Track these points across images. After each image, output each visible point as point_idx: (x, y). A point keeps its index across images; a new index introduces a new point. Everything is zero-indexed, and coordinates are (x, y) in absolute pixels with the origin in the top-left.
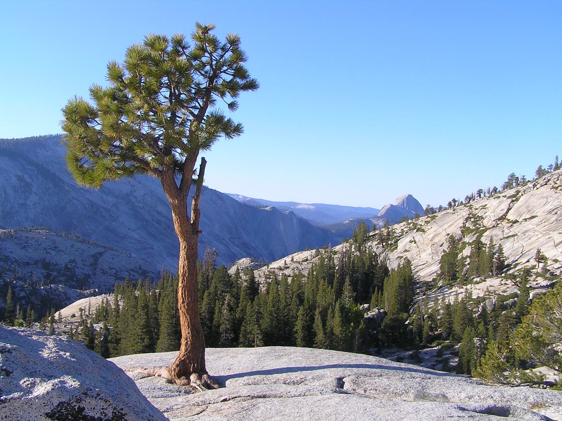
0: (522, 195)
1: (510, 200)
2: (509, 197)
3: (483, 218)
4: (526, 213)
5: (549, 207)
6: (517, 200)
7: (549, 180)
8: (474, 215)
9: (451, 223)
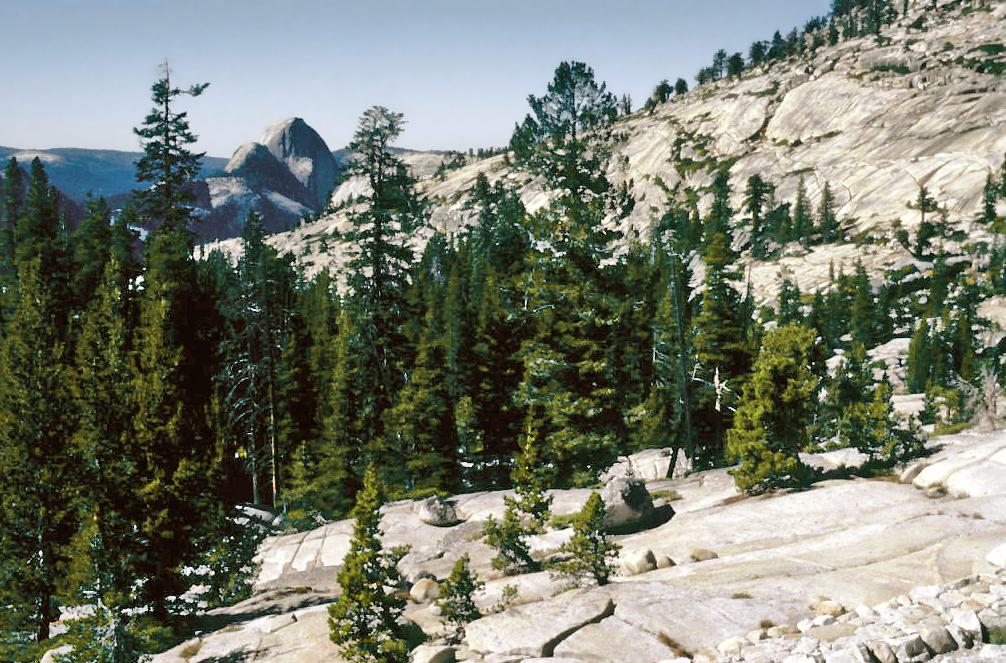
0: (787, 91)
1: (765, 100)
2: (762, 94)
3: (713, 139)
4: (811, 126)
5: (859, 114)
6: (779, 100)
7: (835, 61)
8: (690, 136)
9: (644, 153)
